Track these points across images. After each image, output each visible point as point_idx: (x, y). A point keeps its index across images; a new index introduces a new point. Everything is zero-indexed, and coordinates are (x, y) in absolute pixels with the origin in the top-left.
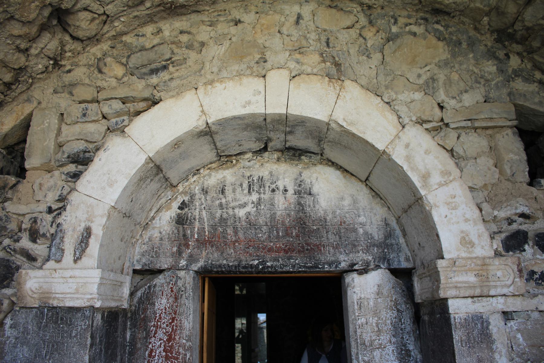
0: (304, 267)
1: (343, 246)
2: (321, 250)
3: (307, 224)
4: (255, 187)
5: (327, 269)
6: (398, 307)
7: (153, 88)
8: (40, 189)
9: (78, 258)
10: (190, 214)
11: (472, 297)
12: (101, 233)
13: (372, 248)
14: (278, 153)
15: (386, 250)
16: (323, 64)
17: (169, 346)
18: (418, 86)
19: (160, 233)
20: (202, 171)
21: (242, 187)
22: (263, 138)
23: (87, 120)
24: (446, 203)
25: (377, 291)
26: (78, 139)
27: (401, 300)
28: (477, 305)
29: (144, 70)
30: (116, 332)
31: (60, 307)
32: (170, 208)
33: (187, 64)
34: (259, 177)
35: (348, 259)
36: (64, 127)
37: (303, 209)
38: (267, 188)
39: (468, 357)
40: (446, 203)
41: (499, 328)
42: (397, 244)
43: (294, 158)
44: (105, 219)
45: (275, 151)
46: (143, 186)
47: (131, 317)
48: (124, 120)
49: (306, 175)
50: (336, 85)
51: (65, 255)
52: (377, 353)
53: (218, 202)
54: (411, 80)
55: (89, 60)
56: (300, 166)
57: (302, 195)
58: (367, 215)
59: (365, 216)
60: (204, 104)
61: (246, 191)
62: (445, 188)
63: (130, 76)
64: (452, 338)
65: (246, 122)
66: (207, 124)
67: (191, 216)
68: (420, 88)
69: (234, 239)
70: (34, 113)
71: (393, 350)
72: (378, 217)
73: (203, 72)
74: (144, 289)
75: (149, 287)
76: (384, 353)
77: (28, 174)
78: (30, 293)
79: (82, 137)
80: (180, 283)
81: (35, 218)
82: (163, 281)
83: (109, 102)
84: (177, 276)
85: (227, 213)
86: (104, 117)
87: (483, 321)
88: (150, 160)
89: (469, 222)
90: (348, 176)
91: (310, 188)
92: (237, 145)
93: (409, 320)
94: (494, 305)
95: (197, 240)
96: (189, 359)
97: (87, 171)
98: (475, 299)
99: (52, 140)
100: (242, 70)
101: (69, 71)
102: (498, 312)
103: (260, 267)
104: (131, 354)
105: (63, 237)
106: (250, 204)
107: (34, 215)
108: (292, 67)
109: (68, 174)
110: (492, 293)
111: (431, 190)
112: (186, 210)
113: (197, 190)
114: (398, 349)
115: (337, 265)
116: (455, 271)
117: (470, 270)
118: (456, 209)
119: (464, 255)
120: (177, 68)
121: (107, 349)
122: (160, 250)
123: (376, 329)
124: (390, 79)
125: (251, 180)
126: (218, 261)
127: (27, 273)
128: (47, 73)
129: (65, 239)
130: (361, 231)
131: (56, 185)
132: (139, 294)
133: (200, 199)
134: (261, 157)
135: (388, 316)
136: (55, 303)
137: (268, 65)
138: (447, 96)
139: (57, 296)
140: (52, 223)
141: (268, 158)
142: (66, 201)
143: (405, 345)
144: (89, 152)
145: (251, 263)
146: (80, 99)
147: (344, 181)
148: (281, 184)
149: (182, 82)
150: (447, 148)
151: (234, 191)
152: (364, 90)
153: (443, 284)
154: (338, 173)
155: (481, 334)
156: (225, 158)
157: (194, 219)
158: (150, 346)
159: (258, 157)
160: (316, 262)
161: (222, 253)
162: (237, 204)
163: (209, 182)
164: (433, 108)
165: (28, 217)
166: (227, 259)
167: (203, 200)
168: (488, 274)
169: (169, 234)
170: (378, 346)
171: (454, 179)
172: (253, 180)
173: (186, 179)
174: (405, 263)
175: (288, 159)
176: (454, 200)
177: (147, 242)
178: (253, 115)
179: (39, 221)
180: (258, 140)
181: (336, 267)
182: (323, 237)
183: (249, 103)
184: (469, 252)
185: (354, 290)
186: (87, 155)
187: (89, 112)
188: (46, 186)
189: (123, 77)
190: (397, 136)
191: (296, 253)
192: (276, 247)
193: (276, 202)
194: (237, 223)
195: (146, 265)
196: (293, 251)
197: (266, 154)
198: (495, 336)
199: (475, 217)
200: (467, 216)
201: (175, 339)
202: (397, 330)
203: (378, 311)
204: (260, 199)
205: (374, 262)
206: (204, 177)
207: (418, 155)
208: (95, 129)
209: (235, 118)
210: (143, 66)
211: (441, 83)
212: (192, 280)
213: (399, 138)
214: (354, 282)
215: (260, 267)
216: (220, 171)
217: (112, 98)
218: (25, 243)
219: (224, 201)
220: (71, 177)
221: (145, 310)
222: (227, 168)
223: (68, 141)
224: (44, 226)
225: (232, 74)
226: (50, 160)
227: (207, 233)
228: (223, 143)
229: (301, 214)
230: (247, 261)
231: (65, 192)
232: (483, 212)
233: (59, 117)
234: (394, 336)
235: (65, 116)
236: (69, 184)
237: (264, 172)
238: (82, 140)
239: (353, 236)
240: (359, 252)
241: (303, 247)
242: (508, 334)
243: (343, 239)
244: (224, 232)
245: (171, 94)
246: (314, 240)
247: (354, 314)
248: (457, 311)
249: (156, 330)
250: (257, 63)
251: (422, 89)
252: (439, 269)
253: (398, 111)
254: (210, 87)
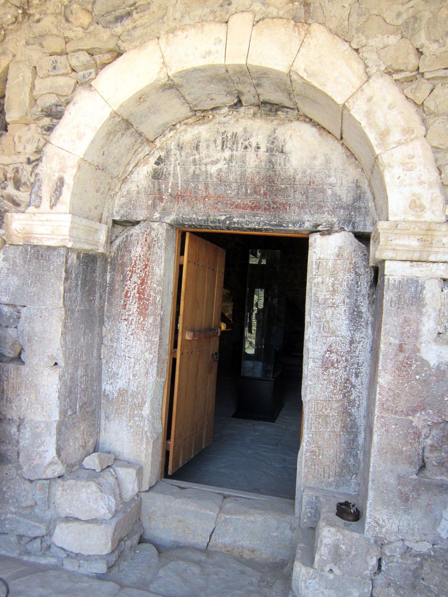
0: (269, 224)
1: (309, 206)
2: (286, 209)
3: (276, 183)
4: (228, 144)
5: (291, 228)
6: (357, 270)
7: (118, 38)
8: (20, 141)
9: (53, 205)
10: (165, 169)
11: (412, 261)
12: (72, 183)
13: (338, 210)
14: (254, 108)
15: (353, 213)
16: (291, 5)
17: (142, 289)
18: (395, 28)
19: (138, 187)
20: (178, 126)
21: (215, 144)
22: (232, 91)
23: (57, 73)
24: (401, 163)
25: (338, 253)
26: (50, 93)
27: (361, 264)
28: (415, 269)
29: (109, 18)
30: (94, 272)
31: (40, 246)
32: (148, 164)
33: (151, 10)
34: (233, 133)
35: (313, 220)
36: (36, 82)
37: (273, 168)
38: (240, 145)
39: (395, 316)
40: (401, 163)
41: (434, 294)
42: (365, 208)
43: (270, 113)
44: (75, 170)
45: (251, 105)
46: (114, 140)
47: (111, 262)
48: (90, 73)
49: (280, 131)
50: (301, 30)
51: (42, 202)
52: (329, 312)
53: (192, 158)
54: (388, 21)
55: (55, 7)
56: (275, 122)
57: (274, 153)
58: (338, 176)
59: (336, 177)
60: (165, 55)
61: (219, 148)
62: (404, 148)
63: (96, 24)
64: (383, 298)
65: (208, 73)
66: (169, 77)
67: (166, 172)
68: (397, 30)
69: (204, 194)
70: (10, 66)
71: (345, 311)
72: (350, 179)
73: (165, 18)
74: (122, 238)
75: (127, 236)
76: (336, 312)
77: (9, 127)
78: (16, 233)
79: (52, 91)
80: (153, 234)
81: (17, 168)
82: (138, 231)
83: (76, 54)
84: (151, 228)
85: (200, 169)
86: (73, 70)
87: (417, 285)
88: (115, 114)
89: (423, 185)
90: (325, 133)
91: (283, 146)
92: (209, 99)
93: (366, 284)
94: (433, 271)
95: (171, 195)
96: (159, 301)
97: (59, 125)
98: (414, 263)
99: (28, 94)
100: (205, 16)
101: (38, 21)
102: (437, 278)
103: (228, 222)
104: (111, 293)
105: (41, 186)
106: (222, 161)
107: (16, 166)
108: (257, 9)
109: (42, 127)
110: (432, 258)
111: (388, 149)
112: (162, 165)
113: (173, 146)
114: (350, 310)
115: (300, 225)
116: (396, 234)
117: (413, 234)
118: (411, 170)
119: (410, 218)
120: (141, 14)
121: (84, 285)
122: (136, 202)
123: (331, 289)
124: (364, 20)
125: (224, 136)
126: (188, 215)
127: (12, 216)
128: (18, 23)
129: (43, 188)
130: (329, 192)
131: (33, 137)
132: (118, 242)
133: (175, 155)
134: (237, 112)
135: (345, 278)
136: (35, 242)
137: (232, 8)
138: (429, 39)
139: (37, 236)
140: (32, 172)
141: (244, 113)
142: (42, 153)
143: (358, 307)
144: (60, 106)
145: (218, 218)
146: (51, 51)
147: (319, 138)
148: (253, 142)
149: (145, 31)
150: (417, 102)
151: (208, 147)
152: (332, 35)
153: (382, 245)
154: (314, 130)
155: (413, 297)
156: (201, 114)
157: (169, 174)
158: (126, 288)
159: (234, 112)
160: (281, 220)
161: (192, 208)
162: (210, 160)
163: (185, 138)
164: (408, 54)
165: (11, 167)
166: (201, 214)
167: (178, 156)
168: (432, 240)
169: (145, 188)
170: (331, 305)
171: (417, 137)
172: (227, 137)
173: (163, 134)
174: (370, 227)
175: (264, 114)
176: (411, 160)
177: (126, 195)
178: (213, 67)
179: (20, 171)
180: (229, 93)
181: (300, 226)
182: (289, 196)
183: (209, 53)
184: (418, 216)
185: (314, 250)
186: (59, 109)
187: (58, 65)
188: (24, 139)
189: (89, 26)
190: (360, 89)
191: (262, 211)
192: (243, 204)
193: (247, 159)
194: (209, 180)
195: (124, 216)
196: (259, 209)
197: (242, 109)
198: (426, 301)
199: (431, 180)
200: (423, 179)
201: (147, 283)
202: (352, 291)
203: (335, 272)
204: (232, 156)
205: (339, 224)
206: (181, 132)
208: (64, 83)
209: (195, 70)
210: (108, 13)
211: (424, 23)
212: (165, 231)
213: (362, 90)
214: (315, 242)
215: (228, 222)
216: (196, 127)
217: (79, 50)
218: (11, 190)
219: (197, 157)
220: (46, 130)
221: (123, 256)
222: (203, 124)
223: (42, 95)
224: (25, 176)
225: (195, 20)
226: (27, 114)
227: (180, 188)
228: (193, 96)
229: (271, 172)
230: (214, 216)
231: (41, 145)
232: (443, 175)
233: (32, 70)
234: (348, 297)
235: (37, 68)
236: (45, 137)
237: (239, 129)
238: (53, 93)
239: (320, 197)
240: (324, 214)
241: (269, 205)
242: (443, 300)
243: (310, 199)
244: (196, 187)
245: (135, 44)
246: (280, 199)
247: (312, 273)
248: (392, 273)
249: (132, 275)
250: (221, 6)
251: (400, 32)
252: (379, 231)
253: (366, 59)
254: (171, 35)
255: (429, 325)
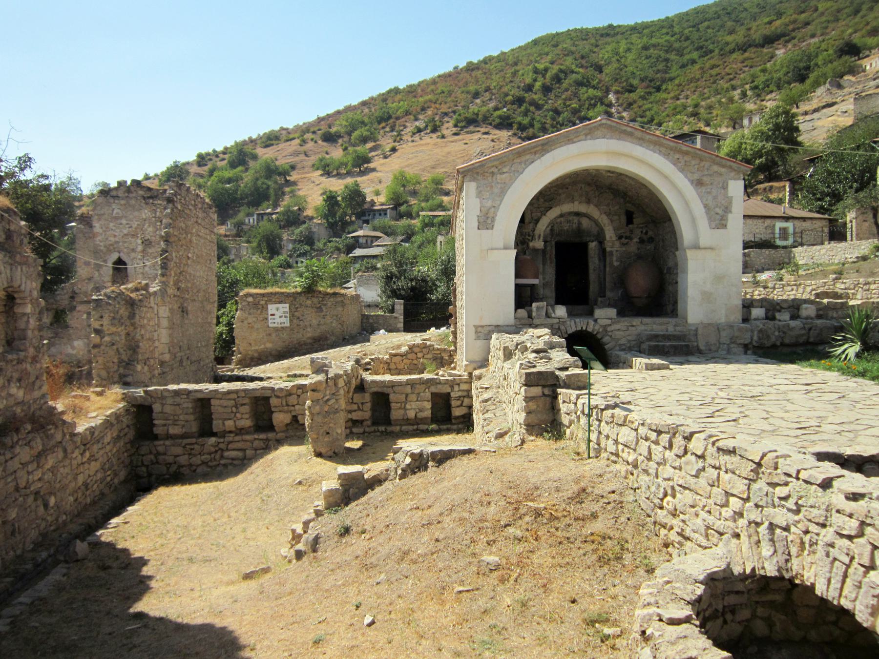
207: (604, 220)
237: (571, 218)
255: (615, 259)
